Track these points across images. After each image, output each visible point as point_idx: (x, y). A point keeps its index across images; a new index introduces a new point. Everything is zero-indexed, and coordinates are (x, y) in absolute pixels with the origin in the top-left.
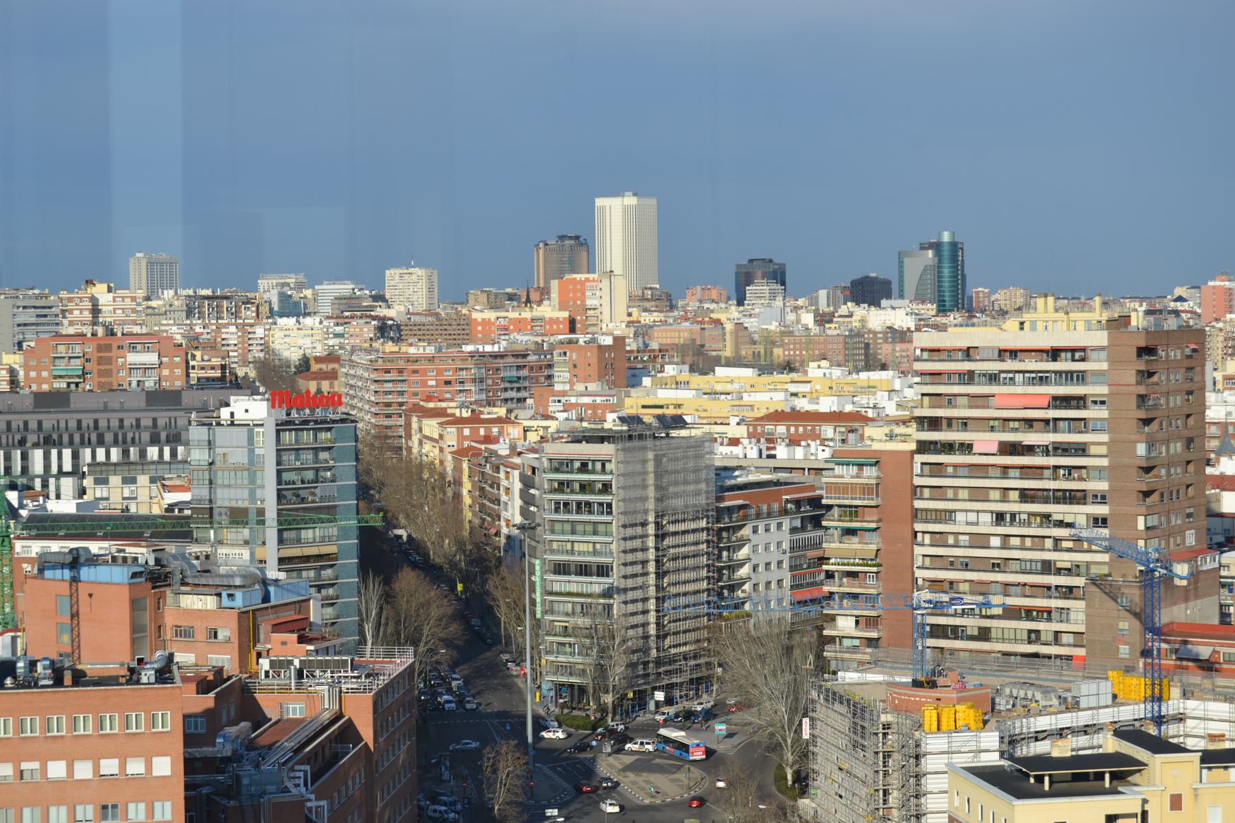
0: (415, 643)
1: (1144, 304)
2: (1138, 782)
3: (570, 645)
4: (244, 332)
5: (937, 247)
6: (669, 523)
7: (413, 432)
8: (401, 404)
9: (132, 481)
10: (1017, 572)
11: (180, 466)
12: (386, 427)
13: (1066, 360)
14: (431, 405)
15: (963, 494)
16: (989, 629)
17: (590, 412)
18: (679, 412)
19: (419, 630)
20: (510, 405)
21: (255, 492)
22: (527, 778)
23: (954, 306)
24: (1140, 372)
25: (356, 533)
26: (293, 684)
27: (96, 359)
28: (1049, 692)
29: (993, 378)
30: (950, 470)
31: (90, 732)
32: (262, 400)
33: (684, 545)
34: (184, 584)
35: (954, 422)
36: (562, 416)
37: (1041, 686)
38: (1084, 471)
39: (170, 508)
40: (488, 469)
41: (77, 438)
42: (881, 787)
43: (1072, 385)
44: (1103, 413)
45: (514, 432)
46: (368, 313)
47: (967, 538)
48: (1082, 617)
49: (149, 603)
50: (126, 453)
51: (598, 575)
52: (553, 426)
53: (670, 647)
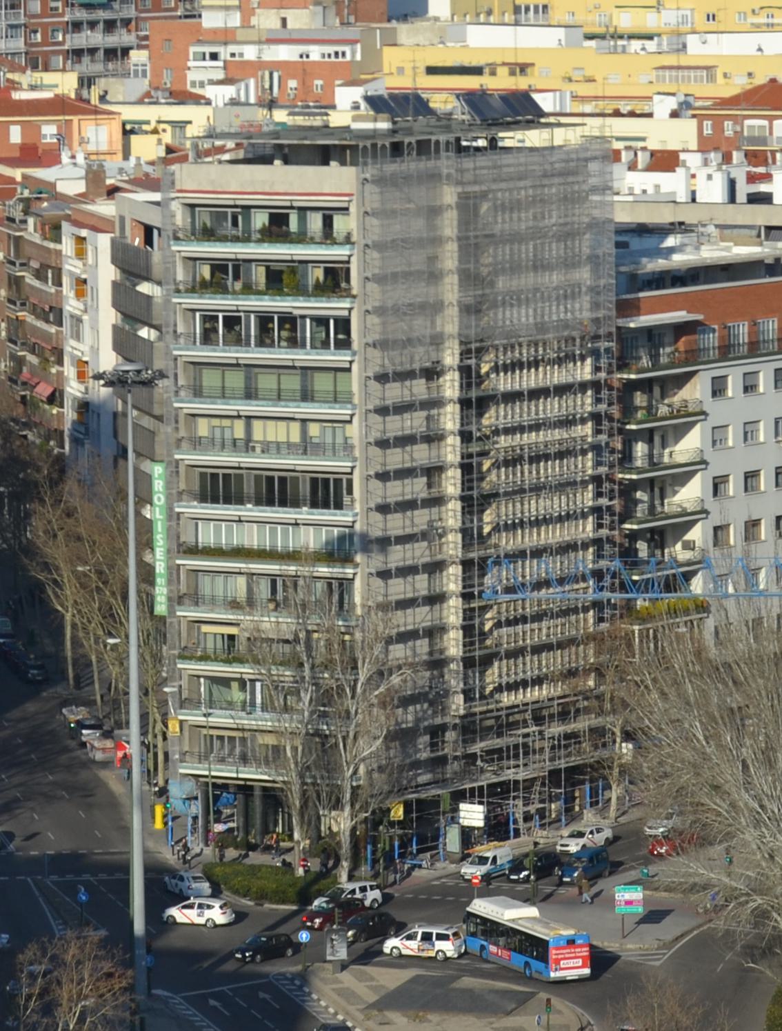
3: (242, 683)
6: (496, 369)
17: (293, 83)
18: (521, 83)
20: (88, 66)
33: (536, 427)
36: (221, 94)
40: (31, 231)
51: (314, 505)
52: (198, 119)
53: (499, 689)
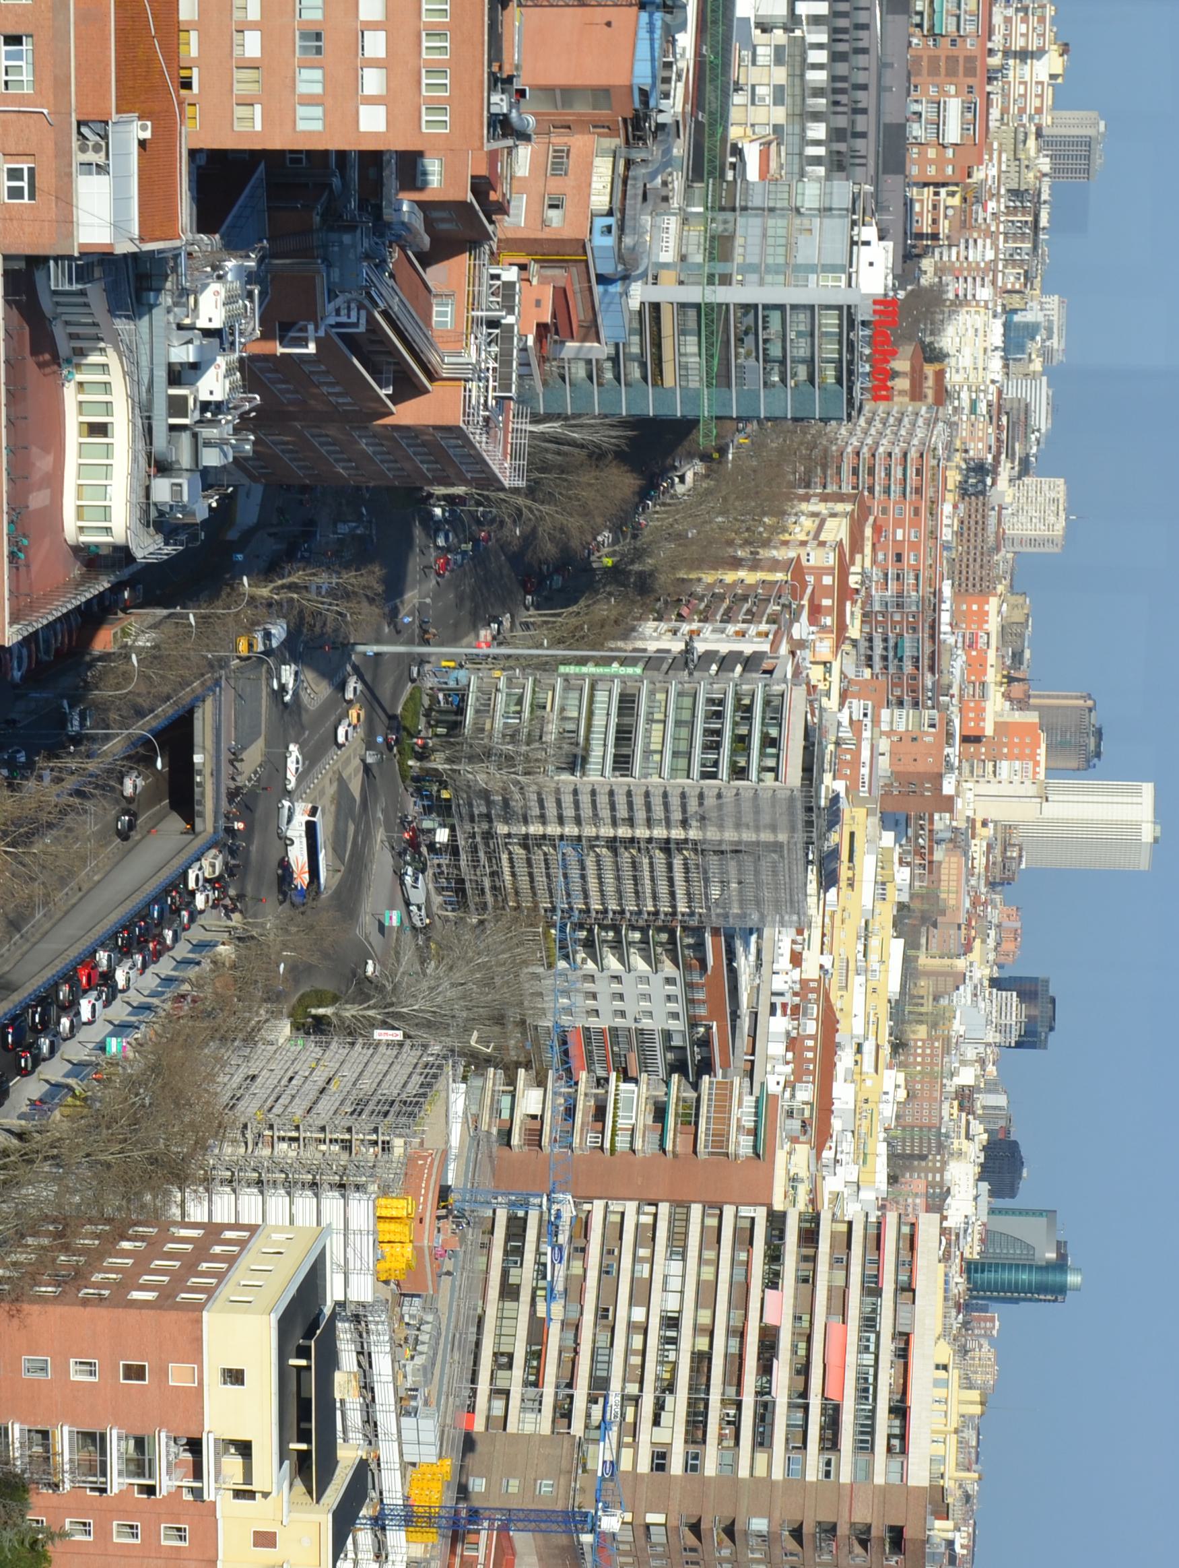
0: (531, 491)
1: (965, 1552)
2: (294, 1489)
3: (519, 712)
4: (985, 271)
5: (1061, 1265)
6: (685, 859)
7: (830, 505)
8: (871, 490)
9: (778, 99)
10: (594, 1342)
11: (796, 169)
12: (839, 468)
13: (890, 1427)
14: (868, 532)
15: (708, 1273)
16: (517, 1299)
17: (848, 757)
18: (843, 883)
19: (550, 498)
20: (863, 644)
21: (754, 272)
22: (334, 643)
23: (975, 1283)
24: (869, 1527)
25: (691, 415)
26: (480, 313)
27: (956, 53)
28: (425, 1375)
29: (869, 1322)
30: (743, 1256)
31: (424, 19)
32: (886, 286)
33: (653, 879)
34: (629, 163)
35: (810, 1265)
36: (844, 717)
37: (433, 1364)
38: (732, 1443)
39: (737, 151)
40: (773, 608)
41: (843, 23)
42: (303, 1135)
43: (854, 1432)
44: (813, 1473)
45: (824, 648)
46: (1004, 450)
47: (646, 1275)
48: (529, 1429)
49: (604, 113)
50: (818, 92)
51: (615, 756)
52: (832, 703)
53: (510, 853)
